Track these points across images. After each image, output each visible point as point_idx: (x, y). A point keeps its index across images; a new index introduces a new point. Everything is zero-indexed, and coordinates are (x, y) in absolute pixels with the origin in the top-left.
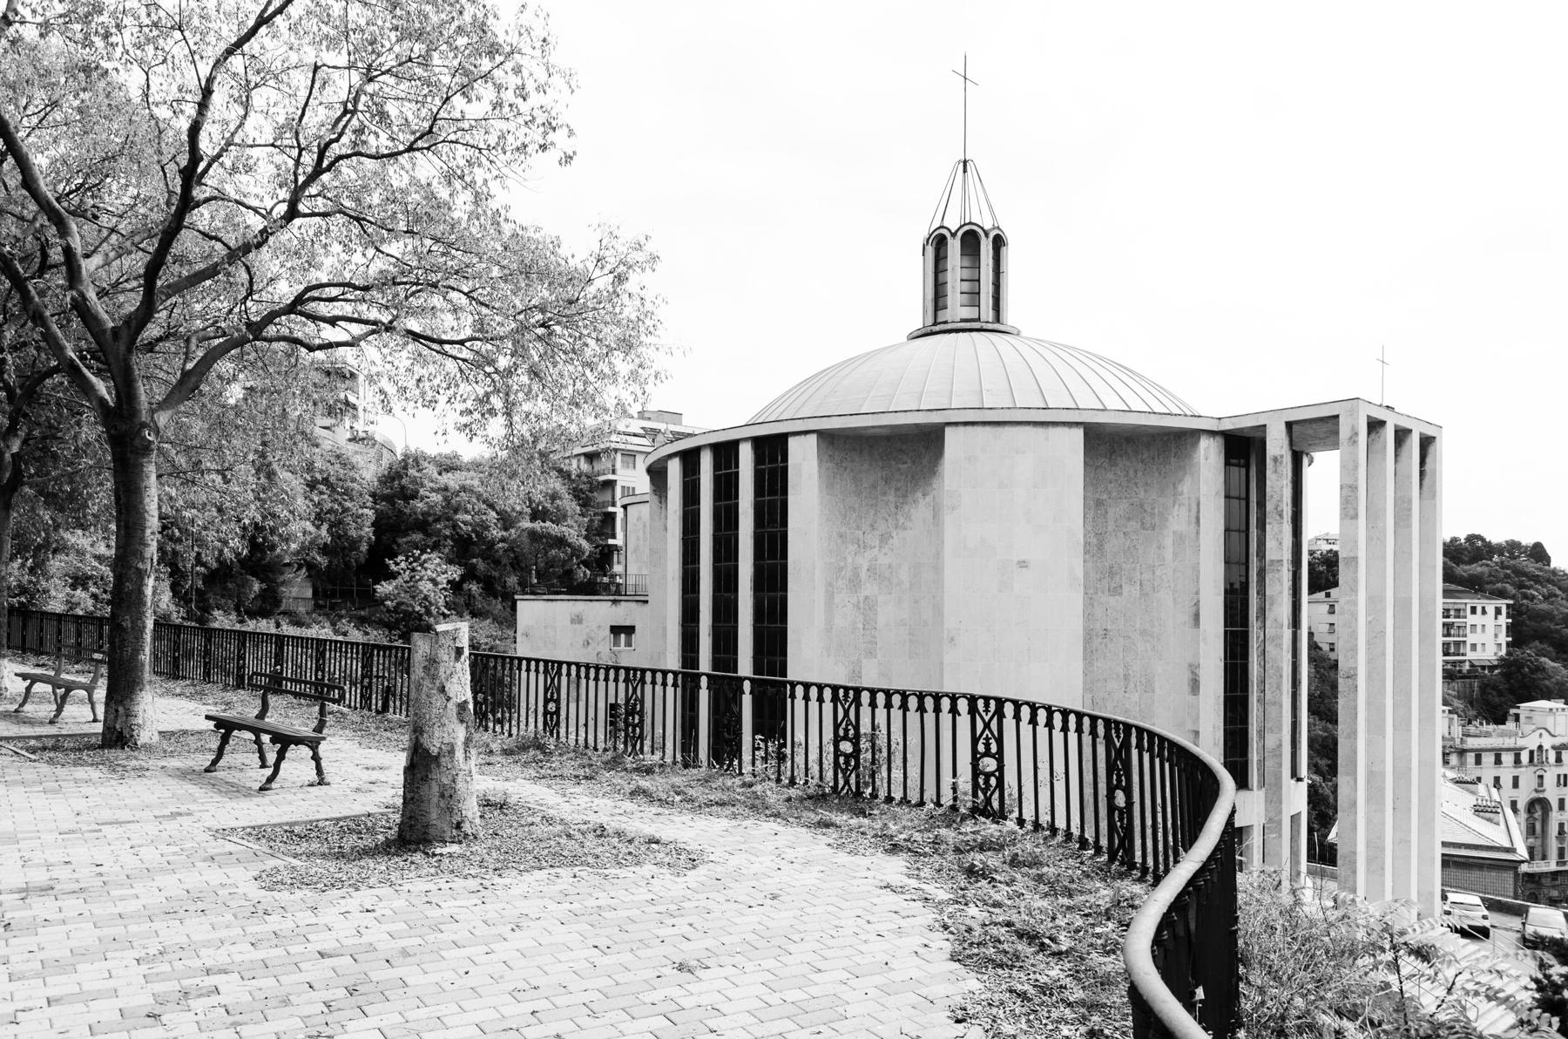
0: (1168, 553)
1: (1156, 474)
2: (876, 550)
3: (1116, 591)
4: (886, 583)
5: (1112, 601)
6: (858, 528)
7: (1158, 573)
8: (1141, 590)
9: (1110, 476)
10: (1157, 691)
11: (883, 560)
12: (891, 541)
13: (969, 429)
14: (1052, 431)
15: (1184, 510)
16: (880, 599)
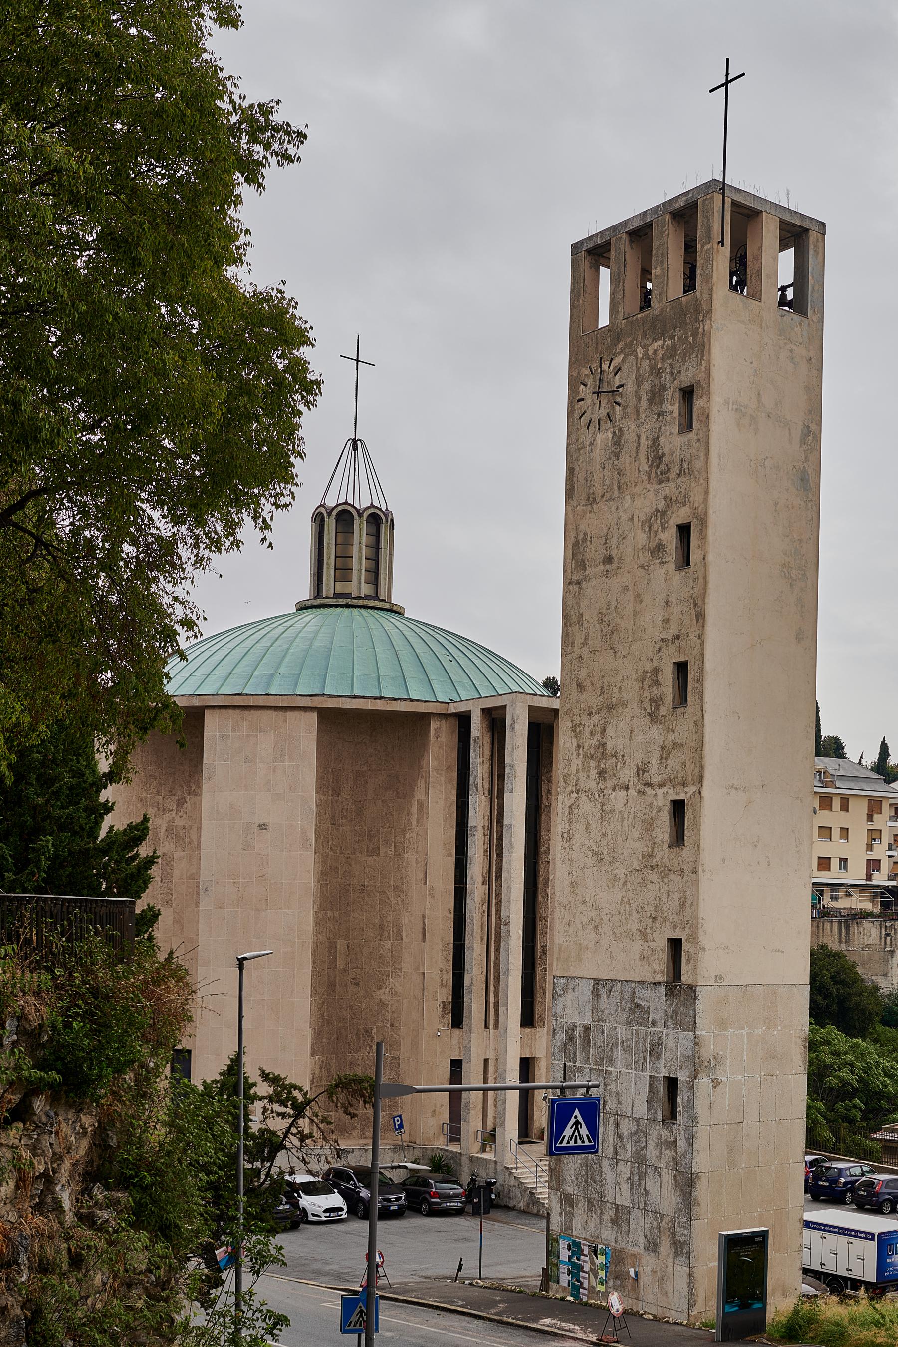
2: (174, 815)
3: (375, 852)
4: (181, 842)
6: (158, 793)
7: (407, 836)
8: (395, 851)
10: (404, 938)
11: (179, 822)
12: (185, 805)
13: (223, 711)
14: (290, 715)
16: (177, 855)
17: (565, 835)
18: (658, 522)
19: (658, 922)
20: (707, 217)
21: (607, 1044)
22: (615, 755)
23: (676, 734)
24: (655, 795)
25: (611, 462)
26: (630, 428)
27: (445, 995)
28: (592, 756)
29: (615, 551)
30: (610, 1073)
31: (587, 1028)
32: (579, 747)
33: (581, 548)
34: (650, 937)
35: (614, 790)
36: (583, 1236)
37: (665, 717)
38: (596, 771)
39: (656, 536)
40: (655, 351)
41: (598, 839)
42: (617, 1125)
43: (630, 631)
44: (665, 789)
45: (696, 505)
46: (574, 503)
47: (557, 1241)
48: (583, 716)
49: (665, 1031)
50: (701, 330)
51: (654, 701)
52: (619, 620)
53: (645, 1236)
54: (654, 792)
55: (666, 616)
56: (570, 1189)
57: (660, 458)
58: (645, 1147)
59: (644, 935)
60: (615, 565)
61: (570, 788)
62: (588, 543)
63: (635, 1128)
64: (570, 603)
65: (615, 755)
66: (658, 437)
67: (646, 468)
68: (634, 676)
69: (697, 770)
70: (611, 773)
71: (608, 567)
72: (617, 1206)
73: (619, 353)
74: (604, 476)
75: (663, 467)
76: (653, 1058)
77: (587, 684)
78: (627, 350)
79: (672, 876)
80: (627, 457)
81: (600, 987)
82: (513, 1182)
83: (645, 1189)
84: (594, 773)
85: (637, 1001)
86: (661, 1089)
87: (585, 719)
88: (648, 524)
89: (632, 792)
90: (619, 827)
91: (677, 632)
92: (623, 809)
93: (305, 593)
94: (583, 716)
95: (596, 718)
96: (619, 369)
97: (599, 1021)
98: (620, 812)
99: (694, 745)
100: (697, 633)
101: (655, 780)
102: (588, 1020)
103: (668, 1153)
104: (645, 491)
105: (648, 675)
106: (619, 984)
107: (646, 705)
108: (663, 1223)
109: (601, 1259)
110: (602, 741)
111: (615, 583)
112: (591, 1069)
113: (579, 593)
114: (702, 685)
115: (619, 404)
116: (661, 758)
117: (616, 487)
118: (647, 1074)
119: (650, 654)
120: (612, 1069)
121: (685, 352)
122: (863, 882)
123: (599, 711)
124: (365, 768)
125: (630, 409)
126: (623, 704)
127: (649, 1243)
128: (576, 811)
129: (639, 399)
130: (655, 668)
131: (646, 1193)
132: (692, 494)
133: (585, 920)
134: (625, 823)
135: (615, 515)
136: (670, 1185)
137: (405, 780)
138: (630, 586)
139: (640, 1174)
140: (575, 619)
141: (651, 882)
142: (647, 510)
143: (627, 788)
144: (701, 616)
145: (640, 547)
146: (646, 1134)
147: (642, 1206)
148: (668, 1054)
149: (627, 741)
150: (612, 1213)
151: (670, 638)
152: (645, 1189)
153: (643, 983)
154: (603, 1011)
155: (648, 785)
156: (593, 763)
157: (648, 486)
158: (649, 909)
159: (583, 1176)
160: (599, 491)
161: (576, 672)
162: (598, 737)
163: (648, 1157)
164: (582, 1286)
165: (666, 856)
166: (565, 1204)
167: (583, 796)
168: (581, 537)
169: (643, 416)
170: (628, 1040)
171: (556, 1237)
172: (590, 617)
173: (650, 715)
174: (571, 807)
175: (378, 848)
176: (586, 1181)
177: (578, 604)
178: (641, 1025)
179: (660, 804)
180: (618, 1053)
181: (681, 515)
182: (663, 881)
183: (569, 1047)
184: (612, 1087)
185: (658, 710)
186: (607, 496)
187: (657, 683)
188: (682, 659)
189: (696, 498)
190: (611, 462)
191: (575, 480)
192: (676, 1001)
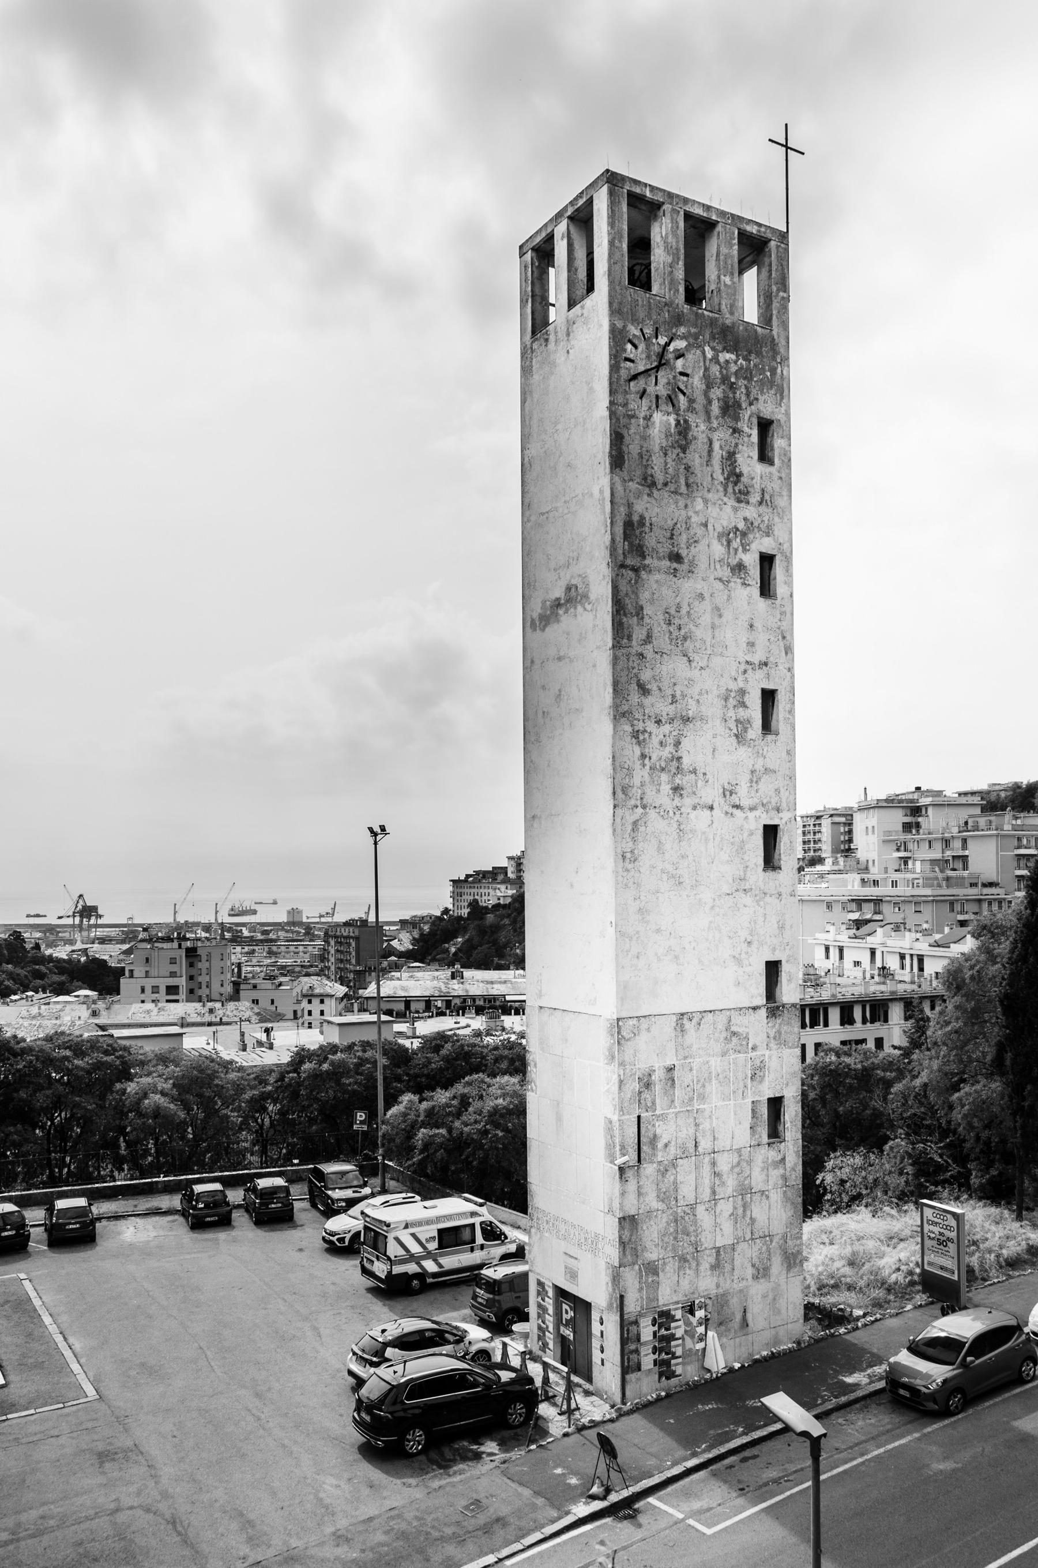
17: (628, 855)
21: (698, 1081)
22: (694, 772)
23: (767, 759)
24: (746, 818)
25: (676, 451)
28: (663, 769)
31: (671, 1069)
32: (643, 756)
35: (694, 808)
37: (754, 741)
38: (669, 786)
42: (714, 1164)
43: (708, 644)
44: (757, 813)
48: (648, 723)
51: (741, 723)
52: (693, 628)
60: (685, 567)
61: (633, 802)
65: (694, 772)
68: (715, 692)
69: (791, 798)
70: (690, 791)
71: (675, 565)
72: (718, 1250)
74: (666, 464)
77: (653, 687)
80: (697, 456)
84: (666, 788)
87: (651, 726)
88: (727, 536)
89: (717, 812)
94: (648, 723)
95: (666, 728)
97: (685, 1058)
98: (704, 833)
99: (787, 772)
101: (745, 803)
106: (710, 1015)
107: (733, 725)
109: (700, 1314)
110: (676, 755)
112: (676, 1114)
115: (684, 394)
116: (751, 781)
117: (682, 481)
119: (734, 673)
125: (699, 405)
138: (707, 595)
150: (712, 1260)
154: (690, 1047)
155: (737, 807)
156: (664, 777)
160: (660, 478)
161: (635, 671)
162: (670, 748)
165: (761, 879)
173: (736, 736)
174: (635, 823)
177: (637, 597)
180: (713, 1089)
184: (706, 1125)
185: (746, 732)
186: (672, 487)
187: (743, 705)
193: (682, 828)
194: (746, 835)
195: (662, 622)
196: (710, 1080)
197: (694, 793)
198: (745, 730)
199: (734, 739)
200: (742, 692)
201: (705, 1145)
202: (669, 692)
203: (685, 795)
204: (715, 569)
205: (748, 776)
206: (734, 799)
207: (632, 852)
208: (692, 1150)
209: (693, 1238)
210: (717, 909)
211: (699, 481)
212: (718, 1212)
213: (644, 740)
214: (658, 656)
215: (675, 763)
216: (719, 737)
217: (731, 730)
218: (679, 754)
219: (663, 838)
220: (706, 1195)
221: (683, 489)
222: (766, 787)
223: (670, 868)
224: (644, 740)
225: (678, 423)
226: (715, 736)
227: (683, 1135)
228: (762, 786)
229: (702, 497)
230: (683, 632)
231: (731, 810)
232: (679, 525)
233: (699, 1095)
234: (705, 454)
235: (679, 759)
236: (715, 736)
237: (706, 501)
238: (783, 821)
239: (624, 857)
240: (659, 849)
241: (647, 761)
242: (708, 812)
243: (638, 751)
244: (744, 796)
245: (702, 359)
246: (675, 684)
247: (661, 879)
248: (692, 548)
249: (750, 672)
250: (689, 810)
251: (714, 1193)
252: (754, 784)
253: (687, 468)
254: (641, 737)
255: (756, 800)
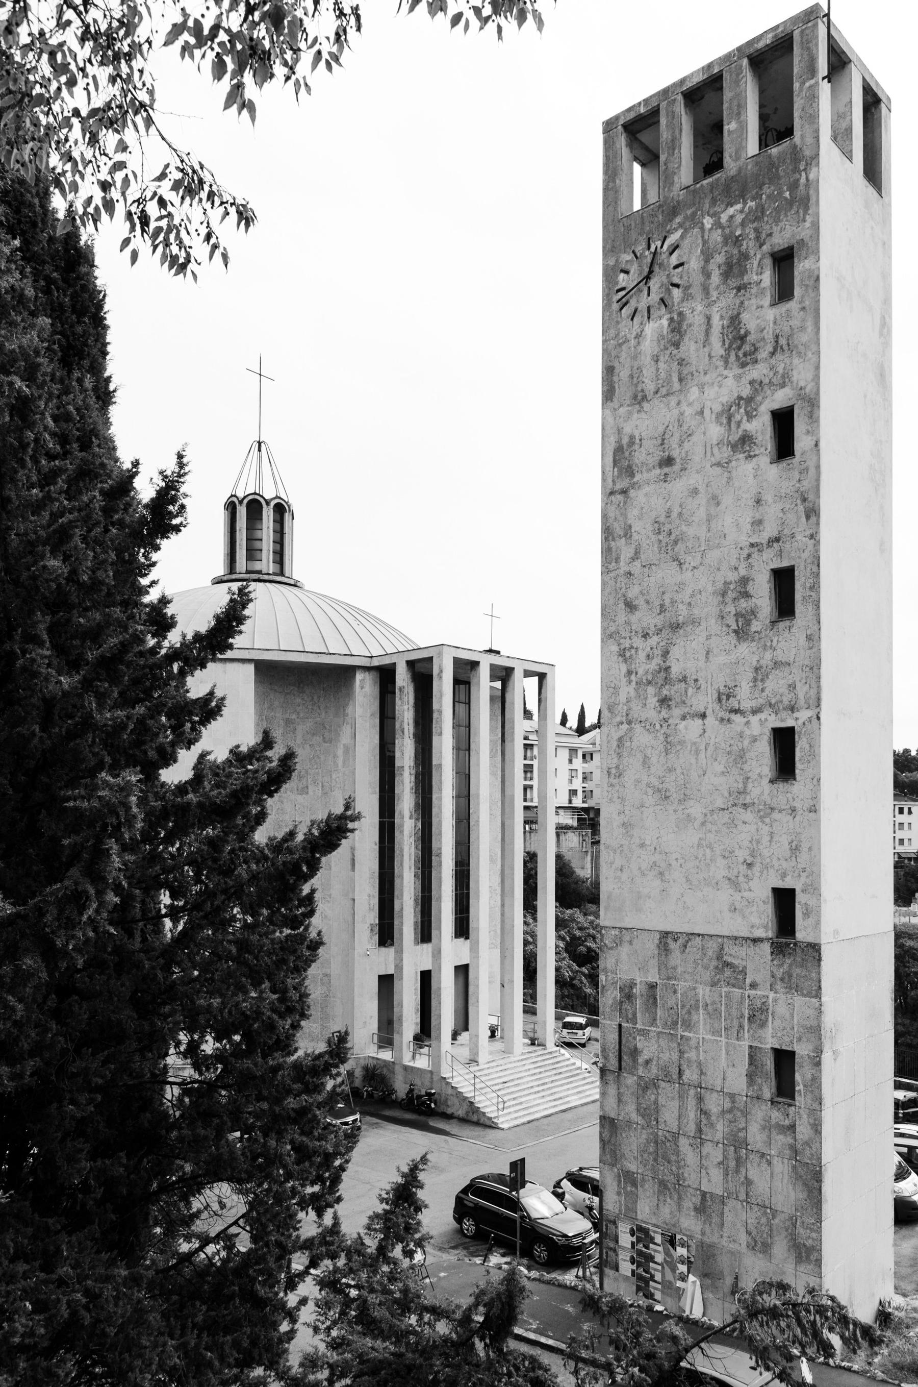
0: (340, 761)
1: (333, 700)
5: (300, 799)
7: (334, 776)
9: (298, 700)
10: (333, 868)
15: (349, 727)
17: (613, 771)
18: (742, 410)
19: (757, 868)
20: (808, 48)
21: (683, 1006)
23: (779, 652)
24: (748, 723)
25: (668, 352)
26: (695, 312)
27: (373, 917)
28: (650, 683)
29: (678, 451)
30: (688, 1039)
31: (652, 987)
32: (629, 673)
33: (627, 454)
34: (744, 886)
35: (684, 718)
36: (654, 1221)
38: (656, 699)
39: (739, 426)
40: (732, 217)
41: (662, 775)
42: (700, 1099)
43: (702, 539)
44: (762, 716)
45: (802, 384)
46: (615, 404)
47: (614, 1223)
48: (635, 639)
49: (772, 995)
50: (803, 180)
51: (742, 616)
52: (684, 528)
53: (749, 1233)
54: (746, 720)
55: (758, 516)
56: (632, 1167)
57: (743, 338)
58: (746, 1129)
59: (734, 883)
60: (677, 467)
61: (618, 719)
62: (636, 447)
63: (728, 1105)
64: (611, 515)
65: (684, 679)
66: (739, 314)
67: (722, 352)
68: (710, 589)
69: (813, 693)
70: (679, 700)
71: (666, 470)
72: (704, 1194)
73: (676, 230)
74: (657, 370)
75: (747, 348)
76: (754, 1026)
77: (640, 602)
78: (687, 224)
79: (776, 815)
81: (669, 941)
82: (450, 1091)
83: (746, 1178)
84: (653, 701)
85: (725, 958)
86: (769, 1063)
87: (638, 642)
88: (727, 415)
89: (710, 720)
90: (693, 761)
91: (775, 534)
92: (698, 740)
93: (220, 569)
94: (635, 639)
95: (653, 641)
96: (677, 247)
97: (669, 978)
98: (695, 743)
99: (807, 662)
100: (808, 533)
101: (746, 705)
102: (653, 977)
103: (782, 1140)
104: (720, 378)
105: (732, 587)
106: (698, 939)
107: (731, 621)
108: (777, 1221)
109: (681, 1251)
110: (664, 666)
111: (678, 487)
112: (659, 1033)
113: (625, 503)
114: (818, 593)
115: (677, 286)
116: (755, 680)
117: (675, 379)
118: (745, 1044)
119: (734, 562)
120: (691, 1035)
121: (778, 210)
122: (567, 805)
123: (659, 631)
124: (294, 717)
125: (696, 290)
126: (696, 622)
127: (756, 1242)
128: (628, 744)
129: (707, 275)
130: (744, 577)
131: (748, 1182)
132: (795, 373)
133: (644, 866)
134: (702, 755)
135: (676, 412)
136: (786, 1177)
137: (331, 726)
138: (701, 489)
139: (738, 1160)
140: (618, 530)
141: (745, 823)
142: (724, 399)
143: (703, 716)
144: (812, 513)
145: (715, 442)
146: (746, 1114)
147: (742, 1196)
148: (778, 1023)
149: (702, 663)
150: (697, 1200)
151: (765, 542)
152: (746, 1178)
153: (736, 938)
154: (675, 968)
155: (736, 711)
156: (651, 690)
157: (726, 372)
158: (742, 855)
159: (650, 1153)
160: (650, 387)
161: (623, 590)
163: (750, 1139)
164: (652, 1278)
165: (767, 792)
166: (625, 1183)
167: (638, 728)
168: (625, 441)
169: (714, 294)
170: (714, 1003)
171: (612, 1218)
172: (642, 529)
173: (735, 631)
174: (620, 740)
175: (307, 787)
176: (655, 1160)
177: (625, 516)
178: (734, 986)
179: (756, 733)
180: (700, 1017)
181: (779, 399)
182: (763, 822)
183: (626, 1006)
184: (692, 1055)
185: (749, 625)
186: (664, 391)
187: (746, 595)
188: (785, 564)
189: (801, 375)
190: (668, 352)
191: (615, 379)
192: (788, 961)
193: (669, 740)
194: (746, 742)
195: (651, 534)
196: (697, 1008)
197: (684, 702)
198: (748, 623)
199: (732, 637)
200: (744, 581)
201: (690, 1075)
202: (657, 603)
203: (673, 706)
204: (712, 454)
205: (750, 675)
206: (733, 703)
207: (617, 767)
208: (675, 1076)
209: (674, 1168)
210: (709, 826)
211: (693, 369)
212: (704, 1153)
213: (631, 657)
214: (646, 570)
215: (663, 674)
216: (713, 638)
217: (728, 626)
218: (668, 664)
219: (649, 752)
220: (691, 1128)
221: (676, 386)
222: (776, 684)
223: (656, 783)
224: (631, 657)
225: (671, 320)
226: (708, 638)
227: (665, 1057)
228: (770, 685)
229: (697, 385)
230: (673, 537)
231: (726, 715)
232: (671, 427)
233: (684, 1022)
234: (702, 337)
235: (667, 669)
236: (708, 638)
237: (701, 387)
238: (800, 722)
239: (609, 773)
240: (644, 763)
241: (633, 677)
242: (700, 721)
243: (624, 668)
244: (745, 697)
245: (699, 237)
246: (664, 593)
247: (646, 794)
248: (686, 443)
249: (755, 555)
250: (678, 721)
251: (700, 1130)
252: (759, 684)
253: (681, 362)
254: (628, 654)
255: (761, 701)
